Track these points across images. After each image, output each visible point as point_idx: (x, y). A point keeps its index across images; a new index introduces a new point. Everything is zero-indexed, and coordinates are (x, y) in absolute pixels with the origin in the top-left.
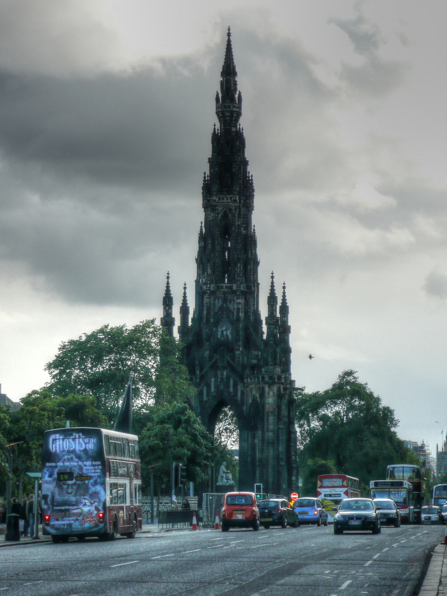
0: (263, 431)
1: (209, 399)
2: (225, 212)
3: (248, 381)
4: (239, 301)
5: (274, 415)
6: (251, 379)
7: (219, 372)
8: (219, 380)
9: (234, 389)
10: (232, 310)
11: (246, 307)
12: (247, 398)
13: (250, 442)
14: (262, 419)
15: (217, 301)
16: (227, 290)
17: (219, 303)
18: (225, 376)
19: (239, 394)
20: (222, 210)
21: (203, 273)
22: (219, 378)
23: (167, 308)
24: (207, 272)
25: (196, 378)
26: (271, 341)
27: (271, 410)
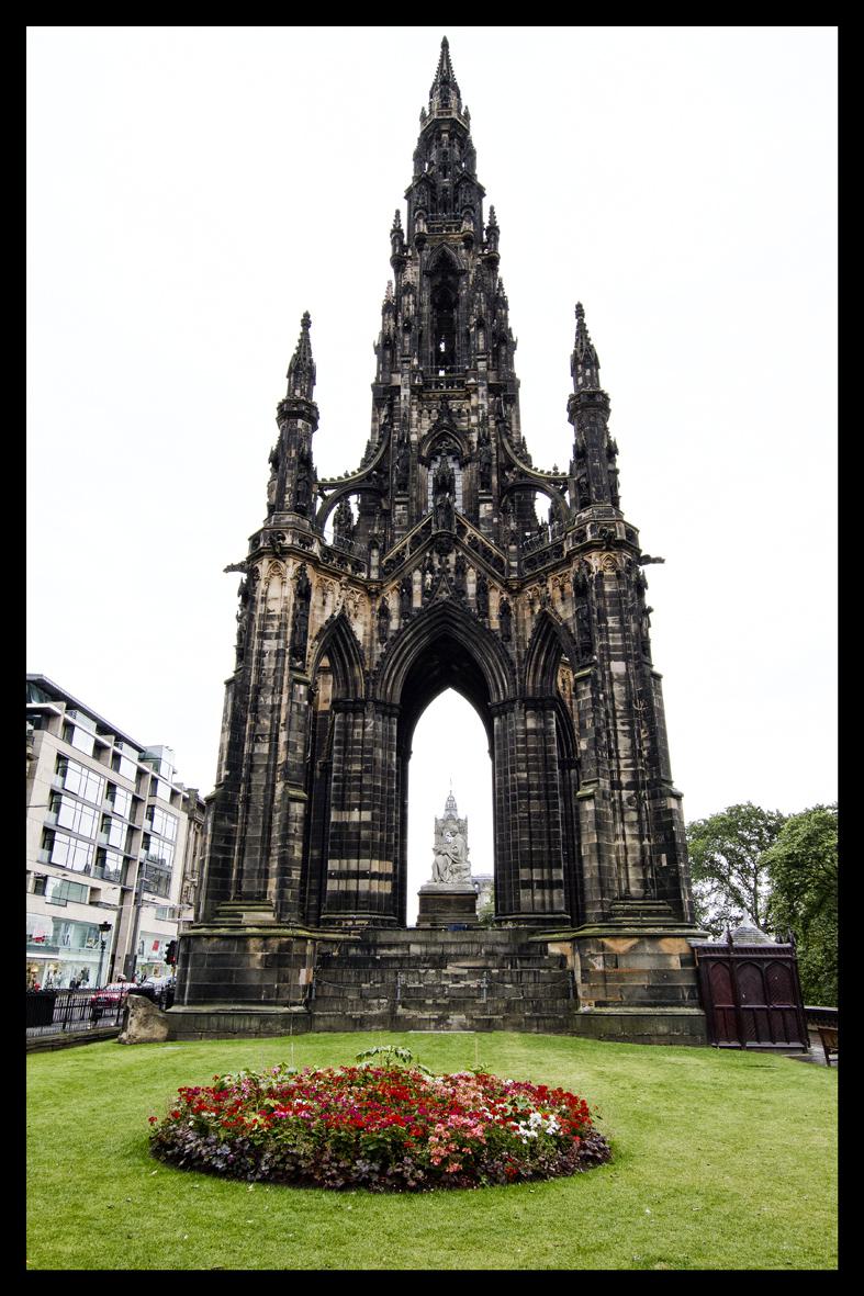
19: (494, 611)
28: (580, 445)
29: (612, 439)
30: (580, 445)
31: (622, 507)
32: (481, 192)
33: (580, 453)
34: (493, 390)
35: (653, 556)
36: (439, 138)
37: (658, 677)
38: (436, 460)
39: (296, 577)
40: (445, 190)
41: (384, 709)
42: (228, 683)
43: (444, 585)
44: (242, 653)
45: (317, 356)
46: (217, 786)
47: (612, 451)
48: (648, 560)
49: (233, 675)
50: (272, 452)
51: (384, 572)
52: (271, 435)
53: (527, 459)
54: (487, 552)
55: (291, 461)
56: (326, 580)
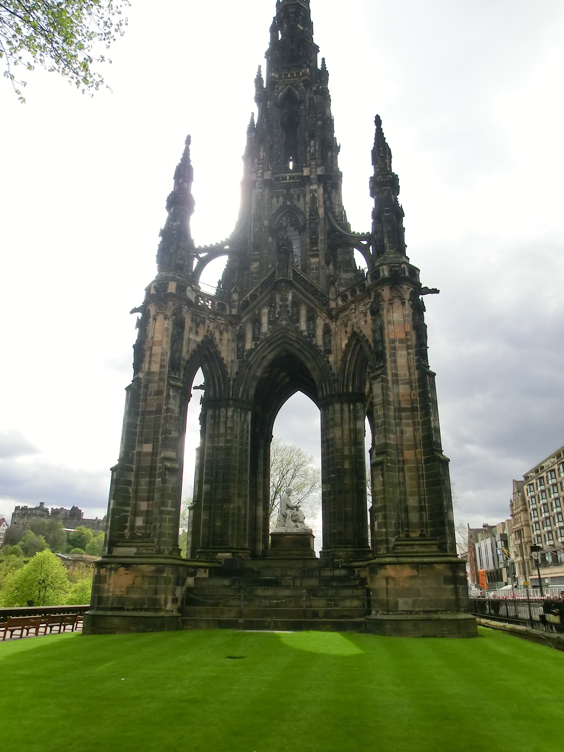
0: (385, 381)
1: (256, 345)
2: (289, 90)
3: (337, 304)
4: (314, 187)
5: (408, 348)
7: (278, 297)
8: (278, 309)
9: (308, 327)
10: (302, 209)
13: (346, 426)
14: (380, 356)
16: (292, 181)
18: (289, 303)
19: (320, 332)
20: (283, 89)
22: (278, 306)
25: (232, 307)
26: (387, 211)
27: (402, 336)
34: (322, 179)
35: (430, 288)
37: (433, 375)
42: (128, 389)
44: (137, 366)
48: (428, 291)
50: (161, 230)
52: (161, 217)
53: (347, 226)
54: (315, 292)
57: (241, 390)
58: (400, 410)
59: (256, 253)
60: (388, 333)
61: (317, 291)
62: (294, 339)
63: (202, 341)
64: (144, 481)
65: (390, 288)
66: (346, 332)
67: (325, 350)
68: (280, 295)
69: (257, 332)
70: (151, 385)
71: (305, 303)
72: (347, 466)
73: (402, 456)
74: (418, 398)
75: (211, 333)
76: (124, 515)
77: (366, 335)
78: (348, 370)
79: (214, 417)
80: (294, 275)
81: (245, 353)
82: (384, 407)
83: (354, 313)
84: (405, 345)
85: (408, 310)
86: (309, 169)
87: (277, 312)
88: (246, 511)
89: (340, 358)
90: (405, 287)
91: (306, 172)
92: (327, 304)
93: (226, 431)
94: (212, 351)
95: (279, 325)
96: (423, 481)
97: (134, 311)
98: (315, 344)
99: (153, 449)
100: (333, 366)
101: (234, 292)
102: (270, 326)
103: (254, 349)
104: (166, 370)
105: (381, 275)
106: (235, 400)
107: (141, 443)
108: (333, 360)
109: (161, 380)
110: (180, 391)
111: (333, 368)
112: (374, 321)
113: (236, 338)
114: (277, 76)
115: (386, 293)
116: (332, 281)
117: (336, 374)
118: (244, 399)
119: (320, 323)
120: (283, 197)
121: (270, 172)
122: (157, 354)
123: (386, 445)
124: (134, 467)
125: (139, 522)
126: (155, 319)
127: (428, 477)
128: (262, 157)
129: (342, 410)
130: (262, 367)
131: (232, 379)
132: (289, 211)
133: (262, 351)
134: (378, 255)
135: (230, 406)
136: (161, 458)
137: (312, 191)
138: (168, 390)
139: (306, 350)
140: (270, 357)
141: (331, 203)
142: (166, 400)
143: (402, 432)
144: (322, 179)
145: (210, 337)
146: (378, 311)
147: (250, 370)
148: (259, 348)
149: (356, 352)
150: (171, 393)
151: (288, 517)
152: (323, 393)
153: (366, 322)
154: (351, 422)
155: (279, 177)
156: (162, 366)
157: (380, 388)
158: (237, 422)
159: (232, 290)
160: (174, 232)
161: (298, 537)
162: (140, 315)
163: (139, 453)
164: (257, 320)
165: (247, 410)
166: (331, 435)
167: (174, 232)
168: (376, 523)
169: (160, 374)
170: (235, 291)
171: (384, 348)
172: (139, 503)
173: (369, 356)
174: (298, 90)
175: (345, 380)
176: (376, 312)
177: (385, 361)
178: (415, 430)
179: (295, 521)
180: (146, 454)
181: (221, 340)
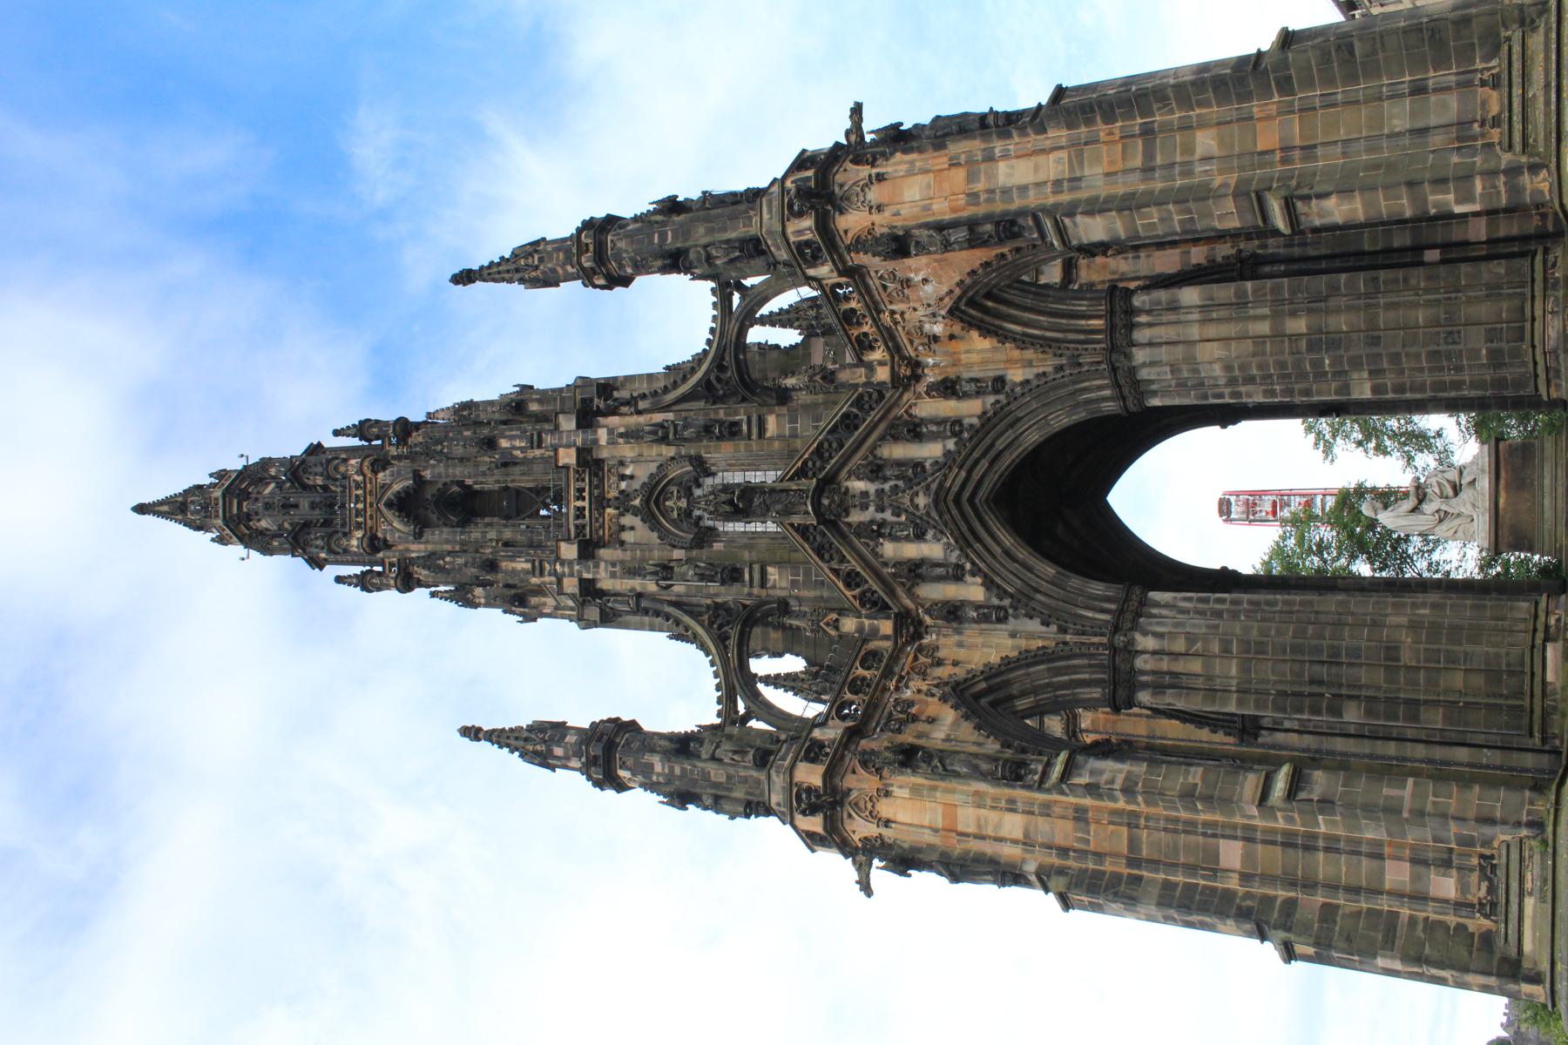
1: (974, 575)
2: (389, 505)
3: (881, 363)
4: (602, 435)
5: (990, 158)
6: (872, 348)
7: (856, 517)
8: (888, 516)
9: (934, 437)
10: (653, 468)
11: (642, 405)
12: (969, 366)
13: (1194, 332)
14: (1008, 227)
15: (628, 536)
16: (586, 494)
17: (637, 531)
18: (871, 488)
21: (540, 591)
22: (879, 516)
23: (558, 751)
24: (523, 570)
26: (663, 237)
27: (960, 174)
28: (659, 263)
29: (651, 208)
30: (659, 263)
31: (764, 184)
32: (315, 449)
33: (675, 262)
34: (587, 418)
35: (848, 124)
36: (249, 517)
37: (1060, 92)
38: (700, 518)
39: (879, 771)
40: (313, 506)
41: (1129, 616)
42: (1066, 904)
43: (906, 500)
44: (1009, 875)
45: (522, 719)
46: (1263, 937)
47: (671, 206)
49: (1051, 895)
51: (878, 607)
52: (641, 803)
54: (848, 422)
55: (688, 770)
56: (891, 714)
57: (1090, 614)
58: (1148, 170)
59: (747, 576)
60: (953, 210)
61: (846, 416)
62: (963, 474)
63: (954, 707)
64: (1322, 865)
65: (841, 213)
66: (952, 337)
67: (996, 391)
68: (852, 511)
69: (940, 571)
70: (1060, 840)
71: (874, 447)
72: (1299, 325)
73: (1273, 151)
74: (1119, 124)
75: (937, 686)
76: (1424, 930)
77: (958, 279)
78: (1046, 329)
79: (1158, 688)
80: (806, 477)
81: (995, 601)
82: (1138, 207)
83: (902, 314)
84: (983, 166)
85: (898, 164)
86: (561, 451)
87: (894, 519)
88: (1424, 605)
89: (1016, 354)
90: (839, 178)
91: (568, 457)
92: (880, 389)
93: (1195, 655)
94: (983, 685)
95: (928, 514)
96: (1340, 93)
97: (866, 888)
98: (980, 417)
99: (1235, 838)
100: (1036, 371)
101: (837, 628)
102: (930, 534)
103: (986, 576)
104: (1019, 793)
105: (808, 236)
106: (1116, 629)
107: (1215, 871)
108: (1020, 372)
109: (1046, 810)
110: (1080, 758)
111: (1041, 370)
112: (922, 249)
113: (955, 625)
114: (359, 534)
115: (852, 222)
116: (823, 378)
117: (1057, 361)
118: (1113, 607)
119: (930, 408)
120: (622, 514)
121: (563, 545)
122: (978, 820)
123: (1239, 193)
124: (1282, 894)
125: (1446, 886)
126: (887, 823)
127: (1329, 81)
128: (529, 566)
129: (1151, 344)
130: (1034, 561)
131: (1060, 636)
132: (657, 502)
133: (990, 559)
134: (763, 253)
135: (1132, 642)
136: (1262, 817)
137: (612, 442)
138: (1074, 789)
139: (992, 445)
140: (1008, 540)
141: (644, 396)
142: (1100, 797)
143: (1206, 159)
144: (587, 418)
145: (947, 689)
146: (895, 238)
147: (1038, 591)
148: (982, 565)
149: (1003, 309)
150: (1083, 779)
151: (1444, 507)
152: (1104, 399)
153: (925, 281)
154: (1182, 318)
155: (577, 527)
156: (1011, 807)
157: (1088, 220)
158: (1176, 625)
159: (833, 633)
160: (677, 771)
161: (1503, 474)
162: (880, 875)
163: (1246, 878)
164: (910, 571)
165: (1144, 602)
166: (1217, 370)
167: (677, 771)
168: (1458, 209)
169: (1032, 813)
170: (836, 625)
171: (988, 218)
172: (1387, 886)
173: (1009, 272)
174: (390, 486)
175: (1071, 336)
176: (899, 245)
177: (1022, 212)
178: (1202, 125)
179: (1457, 489)
180: (1248, 857)
181: (955, 664)
